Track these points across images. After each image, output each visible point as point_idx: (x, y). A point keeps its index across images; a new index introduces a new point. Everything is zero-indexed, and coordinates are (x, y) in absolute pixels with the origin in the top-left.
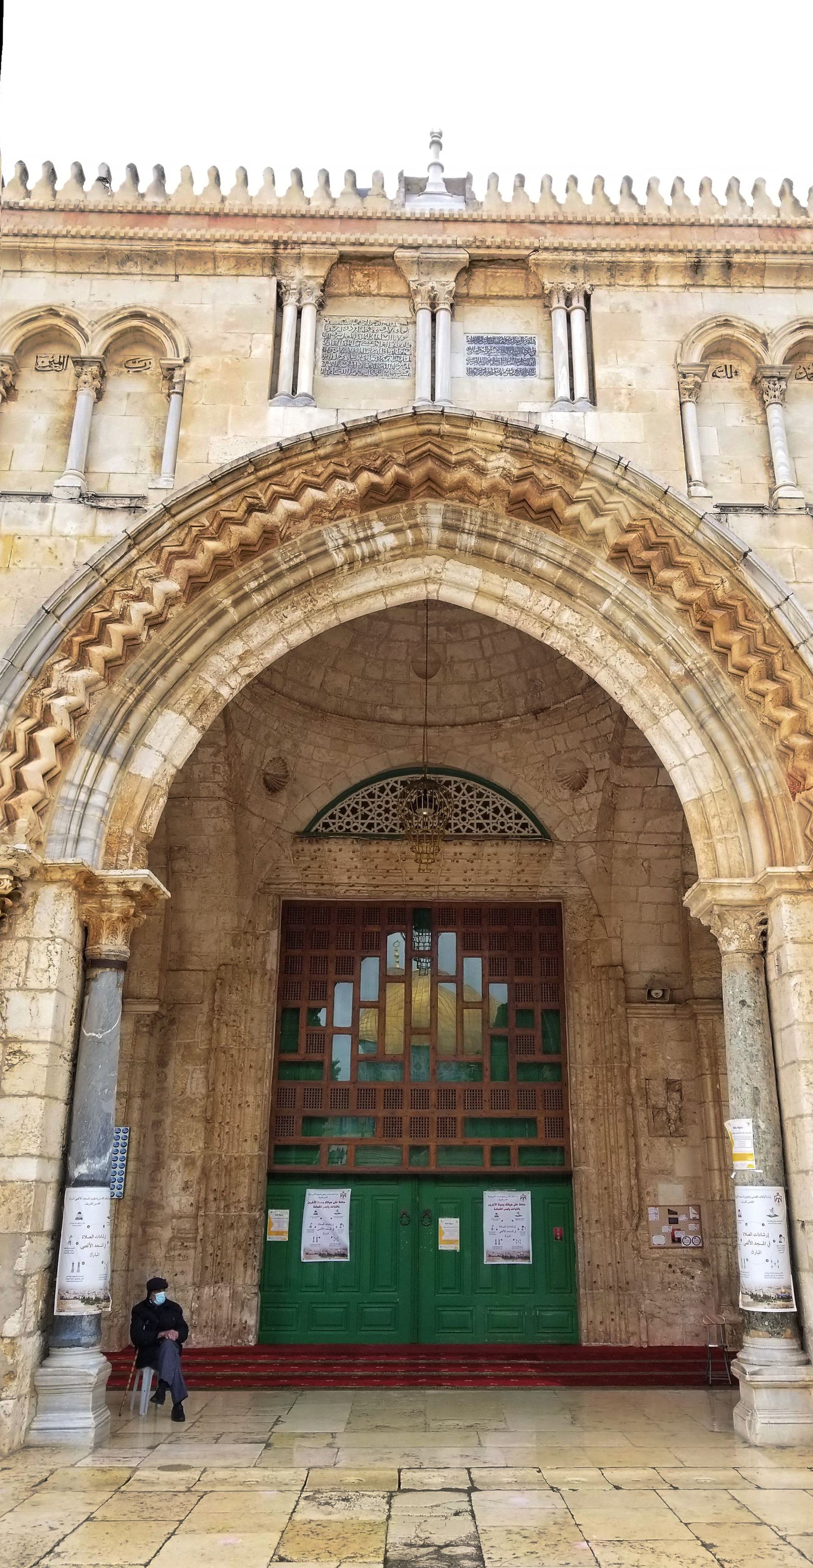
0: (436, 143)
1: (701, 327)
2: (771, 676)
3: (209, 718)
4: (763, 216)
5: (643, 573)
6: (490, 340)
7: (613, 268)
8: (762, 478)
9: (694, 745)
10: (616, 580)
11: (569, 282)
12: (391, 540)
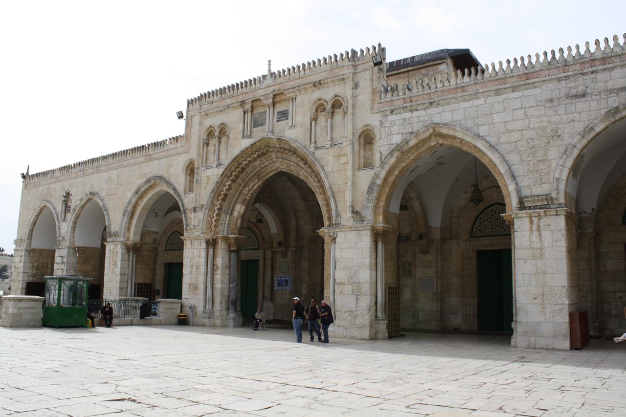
0: (270, 62)
1: (315, 102)
3: (246, 203)
6: (281, 112)
11: (291, 95)
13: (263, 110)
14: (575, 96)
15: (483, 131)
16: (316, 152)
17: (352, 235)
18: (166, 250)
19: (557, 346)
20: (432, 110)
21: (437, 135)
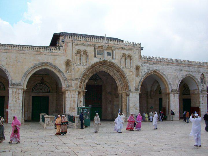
2: (124, 79)
4: (127, 44)
5: (118, 72)
8: (125, 65)
9: (119, 83)
10: (115, 71)
12: (101, 68)
13: (102, 50)
15: (165, 73)
16: (123, 69)
17: (134, 94)
19: (177, 120)
21: (155, 72)
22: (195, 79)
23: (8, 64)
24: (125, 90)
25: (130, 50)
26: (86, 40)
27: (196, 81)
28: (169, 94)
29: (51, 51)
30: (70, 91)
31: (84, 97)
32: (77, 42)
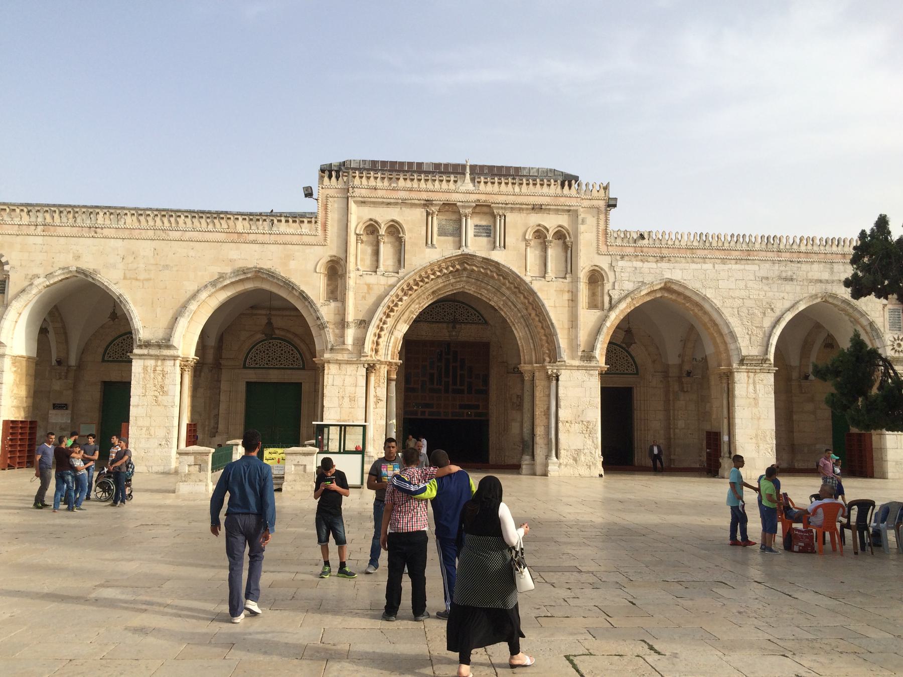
5: (514, 293)
7: (512, 209)
10: (508, 293)
14: (786, 279)
15: (709, 294)
17: (580, 375)
18: (103, 361)
20: (664, 265)
22: (857, 315)
23: (128, 276)
24: (544, 360)
25: (563, 211)
26: (393, 185)
27: (865, 323)
28: (728, 376)
29: (274, 228)
30: (339, 363)
31: (393, 384)
32: (364, 192)
